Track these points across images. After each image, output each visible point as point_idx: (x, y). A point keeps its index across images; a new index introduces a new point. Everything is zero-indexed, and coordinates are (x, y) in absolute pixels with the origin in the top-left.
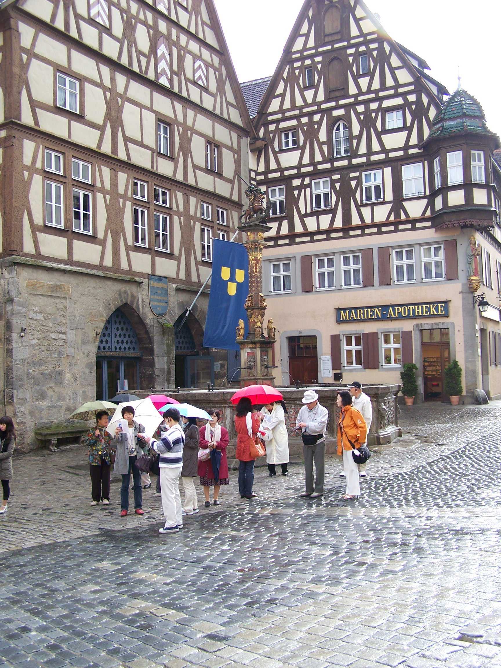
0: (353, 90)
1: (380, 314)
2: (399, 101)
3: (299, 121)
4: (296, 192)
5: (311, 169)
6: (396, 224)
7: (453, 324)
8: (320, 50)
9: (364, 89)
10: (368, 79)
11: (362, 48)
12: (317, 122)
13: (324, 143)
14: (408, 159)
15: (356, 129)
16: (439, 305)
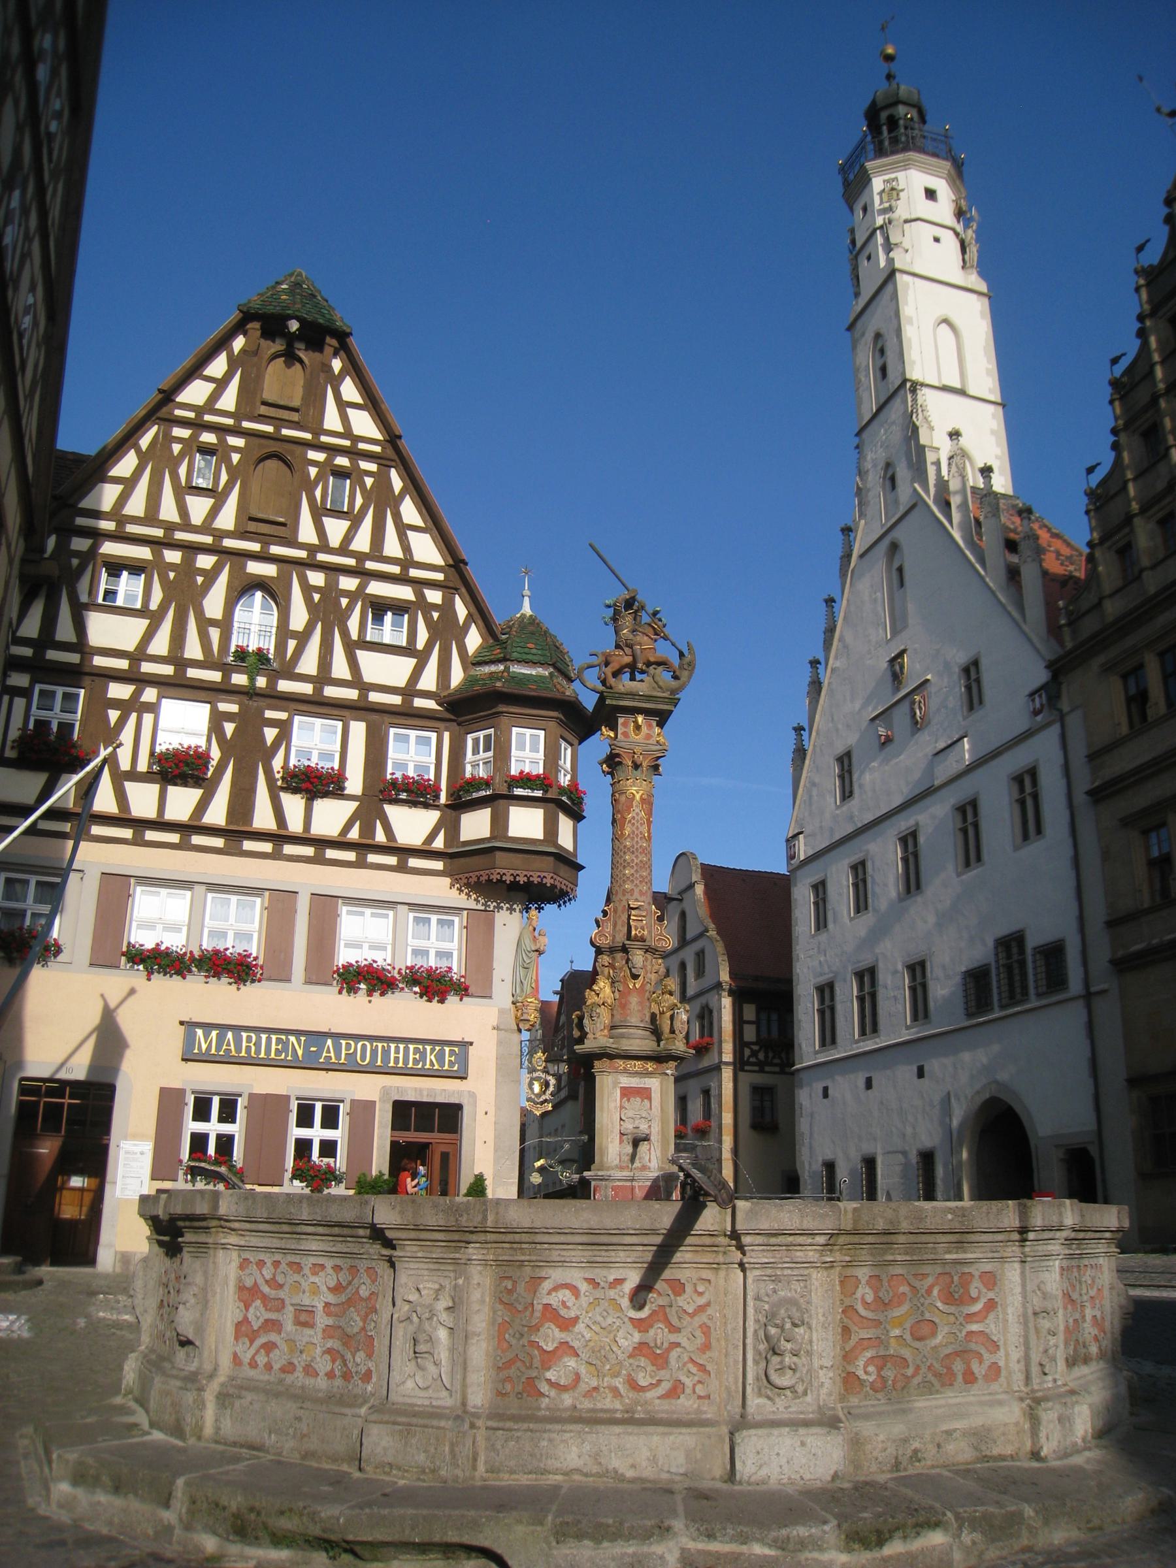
0: (307, 533)
1: (300, 1052)
2: (405, 593)
3: (158, 555)
4: (114, 715)
5: (168, 670)
6: (364, 847)
7: (472, 1095)
8: (246, 424)
9: (335, 541)
10: (345, 525)
11: (342, 461)
12: (202, 572)
13: (213, 623)
14: (407, 716)
15: (299, 617)
16: (447, 1049)
